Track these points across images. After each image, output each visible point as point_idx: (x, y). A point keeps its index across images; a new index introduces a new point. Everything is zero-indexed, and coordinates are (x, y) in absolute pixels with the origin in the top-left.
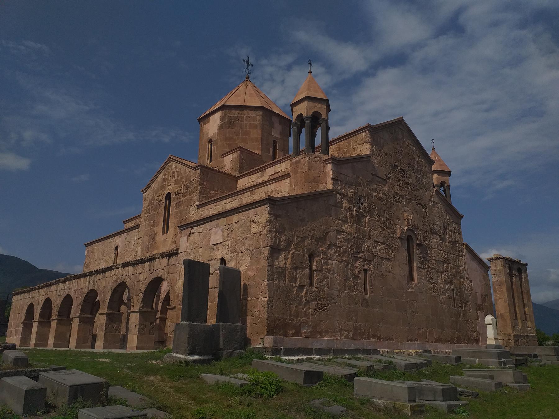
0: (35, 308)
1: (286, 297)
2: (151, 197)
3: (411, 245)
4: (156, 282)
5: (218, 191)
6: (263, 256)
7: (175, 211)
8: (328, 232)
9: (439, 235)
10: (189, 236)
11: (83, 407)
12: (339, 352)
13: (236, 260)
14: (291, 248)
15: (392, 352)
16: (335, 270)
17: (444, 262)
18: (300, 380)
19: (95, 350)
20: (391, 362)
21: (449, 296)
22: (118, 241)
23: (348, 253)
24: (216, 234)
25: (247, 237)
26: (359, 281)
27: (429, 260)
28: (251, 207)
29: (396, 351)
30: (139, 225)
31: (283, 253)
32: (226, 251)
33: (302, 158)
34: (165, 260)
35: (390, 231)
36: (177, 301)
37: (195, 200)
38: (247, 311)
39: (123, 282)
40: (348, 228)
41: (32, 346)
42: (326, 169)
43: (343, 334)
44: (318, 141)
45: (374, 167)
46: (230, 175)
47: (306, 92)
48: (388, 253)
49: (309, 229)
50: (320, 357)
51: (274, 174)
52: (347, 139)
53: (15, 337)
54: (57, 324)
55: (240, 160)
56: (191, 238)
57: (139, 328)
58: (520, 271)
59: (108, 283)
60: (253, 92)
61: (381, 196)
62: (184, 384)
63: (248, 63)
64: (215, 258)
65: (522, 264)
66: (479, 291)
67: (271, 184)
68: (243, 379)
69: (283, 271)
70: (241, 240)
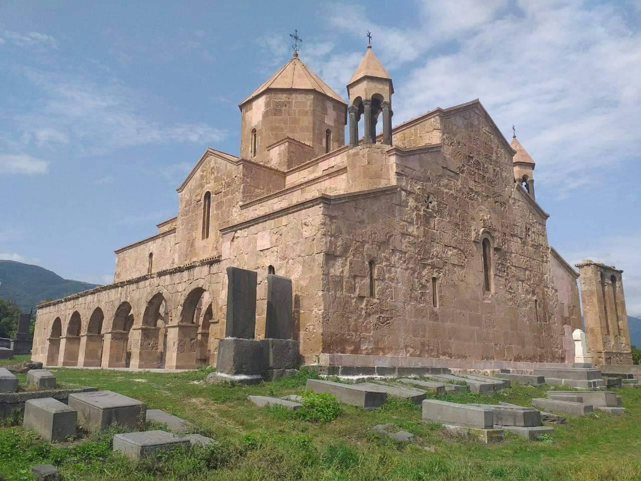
0: (62, 323)
1: (344, 309)
2: (187, 197)
3: (487, 249)
4: (196, 294)
5: (263, 189)
6: (317, 263)
7: (215, 212)
8: (391, 236)
9: (520, 238)
10: (232, 241)
11: (119, 433)
12: (404, 371)
13: (286, 267)
15: (465, 371)
17: (526, 269)
18: (361, 402)
19: (129, 369)
20: (465, 383)
22: (152, 247)
24: (262, 238)
25: (298, 242)
26: (428, 291)
27: (508, 267)
28: (303, 207)
29: (469, 370)
30: (175, 229)
31: (340, 260)
32: (275, 258)
33: (361, 150)
34: (206, 268)
35: (463, 234)
36: (221, 314)
37: (238, 200)
38: (299, 325)
39: (159, 293)
40: (415, 230)
41: (60, 365)
42: (388, 162)
44: (379, 128)
45: (445, 158)
46: (277, 171)
47: (365, 71)
48: (461, 259)
49: (369, 233)
50: (383, 377)
51: (328, 169)
52: (413, 126)
53: (41, 355)
54: (87, 341)
55: (289, 152)
56: (235, 243)
57: (178, 345)
58: (613, 279)
59: (143, 294)
60: (302, 72)
61: (453, 193)
62: (230, 407)
63: (296, 38)
64: (262, 265)
65: (617, 271)
66: (566, 302)
67: (324, 180)
68: (297, 401)
69: (340, 281)
70: (291, 245)
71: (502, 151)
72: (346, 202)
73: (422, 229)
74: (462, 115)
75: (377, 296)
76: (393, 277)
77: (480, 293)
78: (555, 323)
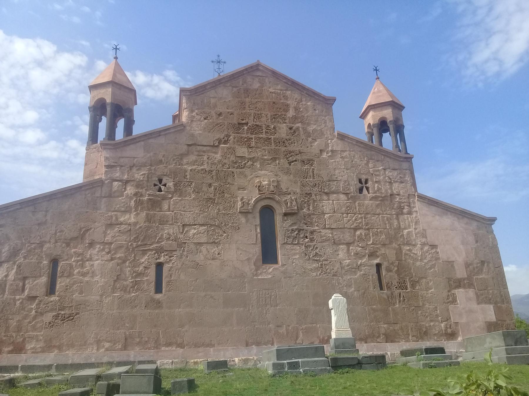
8: (88, 230)
9: (343, 193)
14: (19, 257)
16: (97, 271)
17: (356, 229)
21: (365, 274)
23: (125, 248)
26: (145, 278)
27: (312, 233)
31: (6, 265)
43: (103, 346)
45: (193, 135)
71: (309, 104)
72: (17, 209)
73: (144, 214)
74: (229, 84)
75: (57, 293)
76: (85, 272)
77: (248, 269)
78: (428, 289)
